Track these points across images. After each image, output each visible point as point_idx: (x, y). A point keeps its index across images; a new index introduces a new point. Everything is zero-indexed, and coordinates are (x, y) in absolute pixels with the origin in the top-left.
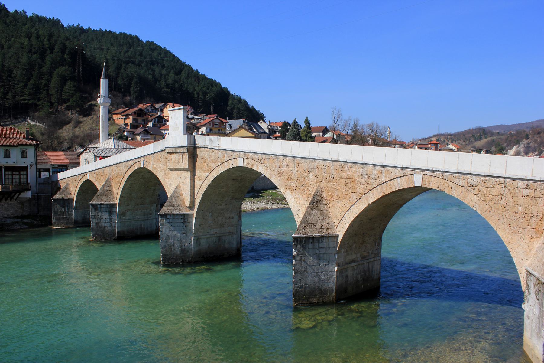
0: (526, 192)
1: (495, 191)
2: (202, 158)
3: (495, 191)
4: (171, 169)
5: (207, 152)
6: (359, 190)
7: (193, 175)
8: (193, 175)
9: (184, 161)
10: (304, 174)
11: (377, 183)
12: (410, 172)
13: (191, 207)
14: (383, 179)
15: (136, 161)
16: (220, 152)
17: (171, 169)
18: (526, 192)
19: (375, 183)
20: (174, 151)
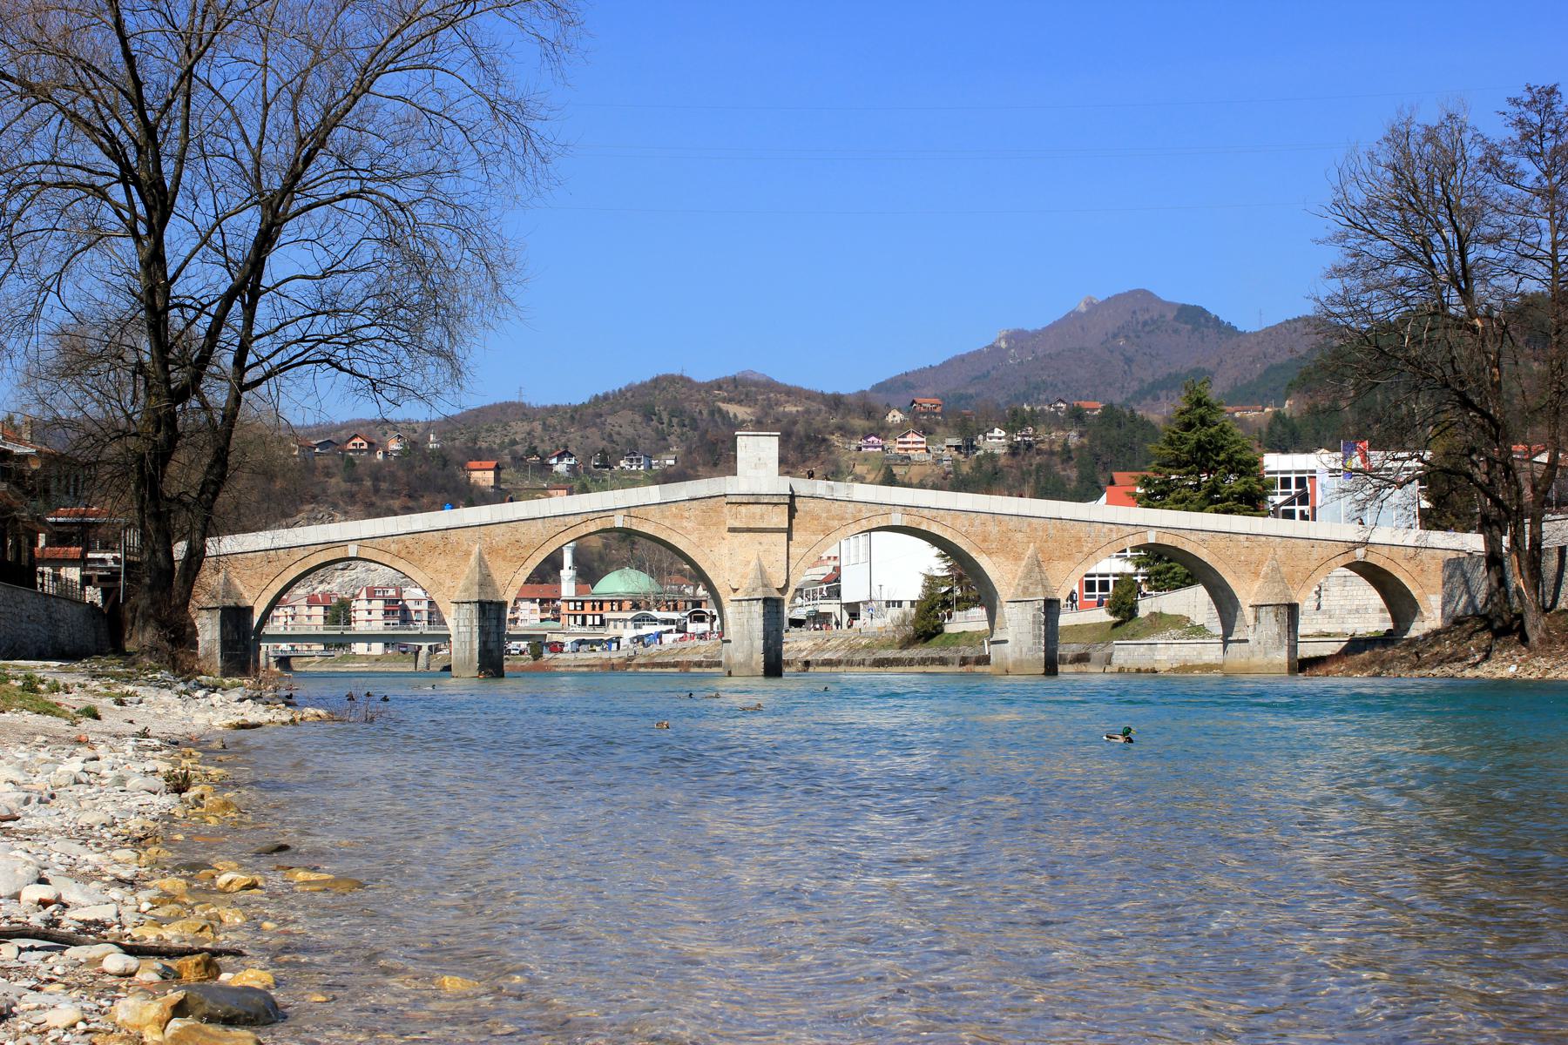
0: (1246, 544)
1: (1222, 544)
2: (806, 512)
3: (1222, 544)
4: (732, 530)
5: (812, 504)
6: (1086, 549)
7: (789, 538)
8: (789, 538)
9: (779, 518)
10: (1010, 534)
11: (1107, 540)
12: (1143, 529)
13: (783, 590)
14: (1114, 536)
15: (596, 515)
16: (851, 505)
17: (732, 530)
18: (1246, 544)
19: (1104, 541)
20: (755, 500)
